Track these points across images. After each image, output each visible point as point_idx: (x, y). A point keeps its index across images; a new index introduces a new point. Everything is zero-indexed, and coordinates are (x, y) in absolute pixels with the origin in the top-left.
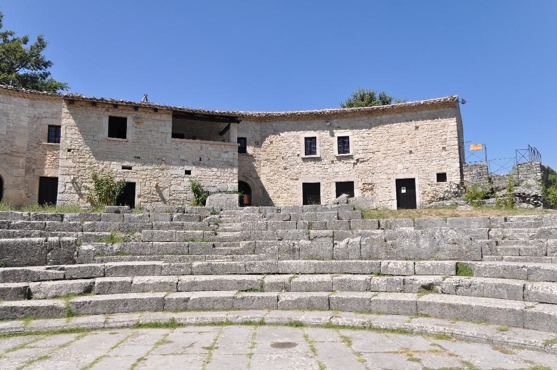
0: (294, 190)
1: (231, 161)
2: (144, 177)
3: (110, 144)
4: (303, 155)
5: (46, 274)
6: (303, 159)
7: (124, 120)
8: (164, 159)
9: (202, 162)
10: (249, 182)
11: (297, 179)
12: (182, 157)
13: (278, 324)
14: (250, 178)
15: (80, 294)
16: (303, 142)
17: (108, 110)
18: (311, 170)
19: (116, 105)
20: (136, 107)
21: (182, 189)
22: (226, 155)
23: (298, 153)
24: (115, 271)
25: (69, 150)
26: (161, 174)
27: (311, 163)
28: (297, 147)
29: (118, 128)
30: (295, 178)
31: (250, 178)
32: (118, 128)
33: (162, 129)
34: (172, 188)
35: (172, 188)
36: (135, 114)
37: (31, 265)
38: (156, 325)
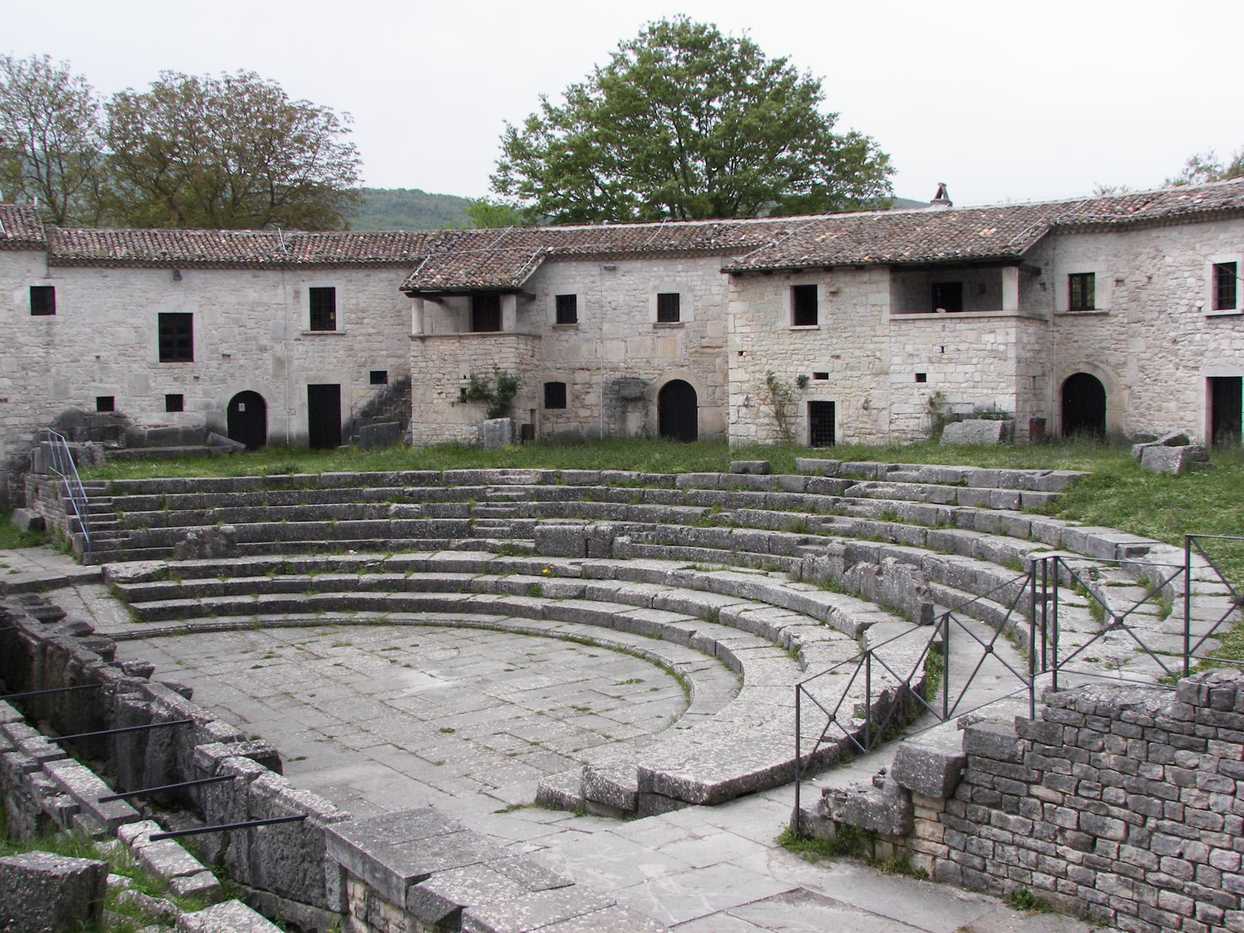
0: (1190, 395)
1: (1002, 348)
2: (847, 391)
3: (794, 335)
4: (1209, 309)
5: (566, 570)
6: (1209, 317)
7: (813, 290)
8: (878, 354)
9: (945, 356)
10: (1099, 375)
11: (1196, 368)
12: (909, 348)
13: (643, 657)
14: (1103, 366)
15: (575, 598)
16: (1209, 274)
17: (788, 278)
18: (1225, 344)
19: (797, 271)
20: (829, 269)
21: (911, 410)
22: (991, 338)
23: (1199, 304)
24: (618, 575)
25: (741, 353)
26: (874, 385)
27: (1226, 326)
28: (1197, 290)
29: (805, 310)
30: (1191, 364)
31: (1103, 366)
32: (805, 310)
33: (873, 299)
34: (895, 409)
35: (895, 409)
36: (828, 278)
37: (555, 556)
38: (234, 628)
